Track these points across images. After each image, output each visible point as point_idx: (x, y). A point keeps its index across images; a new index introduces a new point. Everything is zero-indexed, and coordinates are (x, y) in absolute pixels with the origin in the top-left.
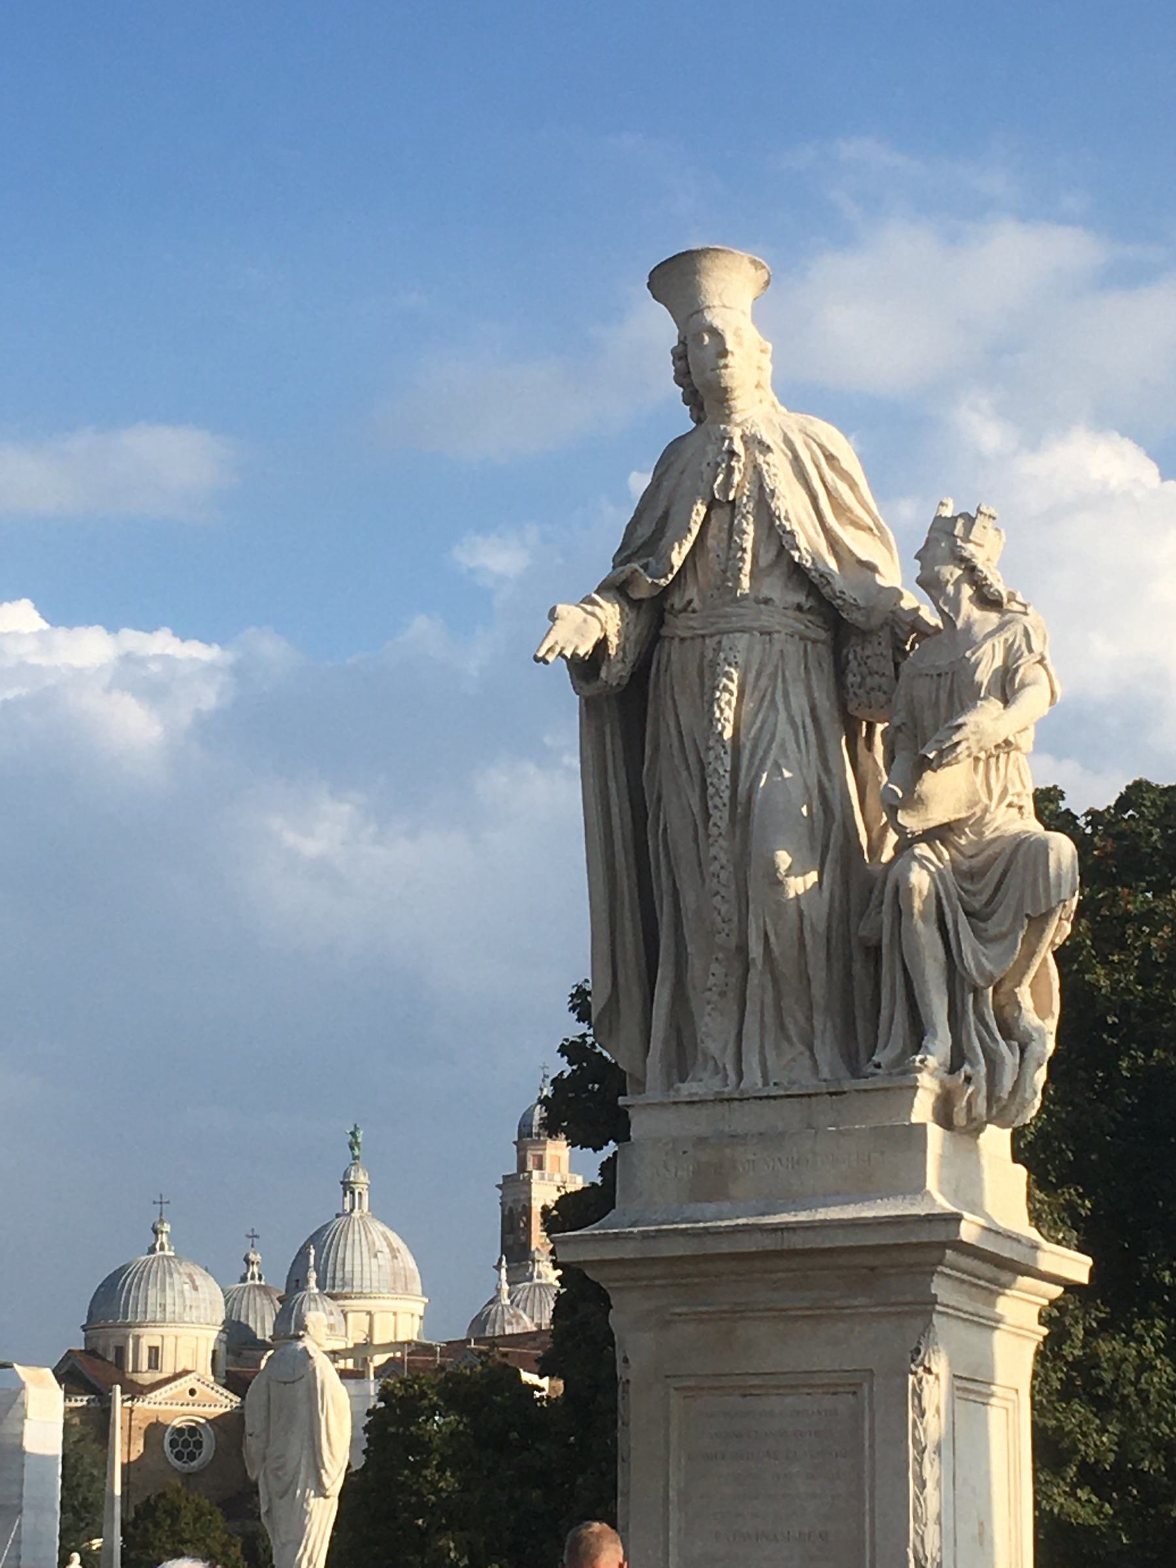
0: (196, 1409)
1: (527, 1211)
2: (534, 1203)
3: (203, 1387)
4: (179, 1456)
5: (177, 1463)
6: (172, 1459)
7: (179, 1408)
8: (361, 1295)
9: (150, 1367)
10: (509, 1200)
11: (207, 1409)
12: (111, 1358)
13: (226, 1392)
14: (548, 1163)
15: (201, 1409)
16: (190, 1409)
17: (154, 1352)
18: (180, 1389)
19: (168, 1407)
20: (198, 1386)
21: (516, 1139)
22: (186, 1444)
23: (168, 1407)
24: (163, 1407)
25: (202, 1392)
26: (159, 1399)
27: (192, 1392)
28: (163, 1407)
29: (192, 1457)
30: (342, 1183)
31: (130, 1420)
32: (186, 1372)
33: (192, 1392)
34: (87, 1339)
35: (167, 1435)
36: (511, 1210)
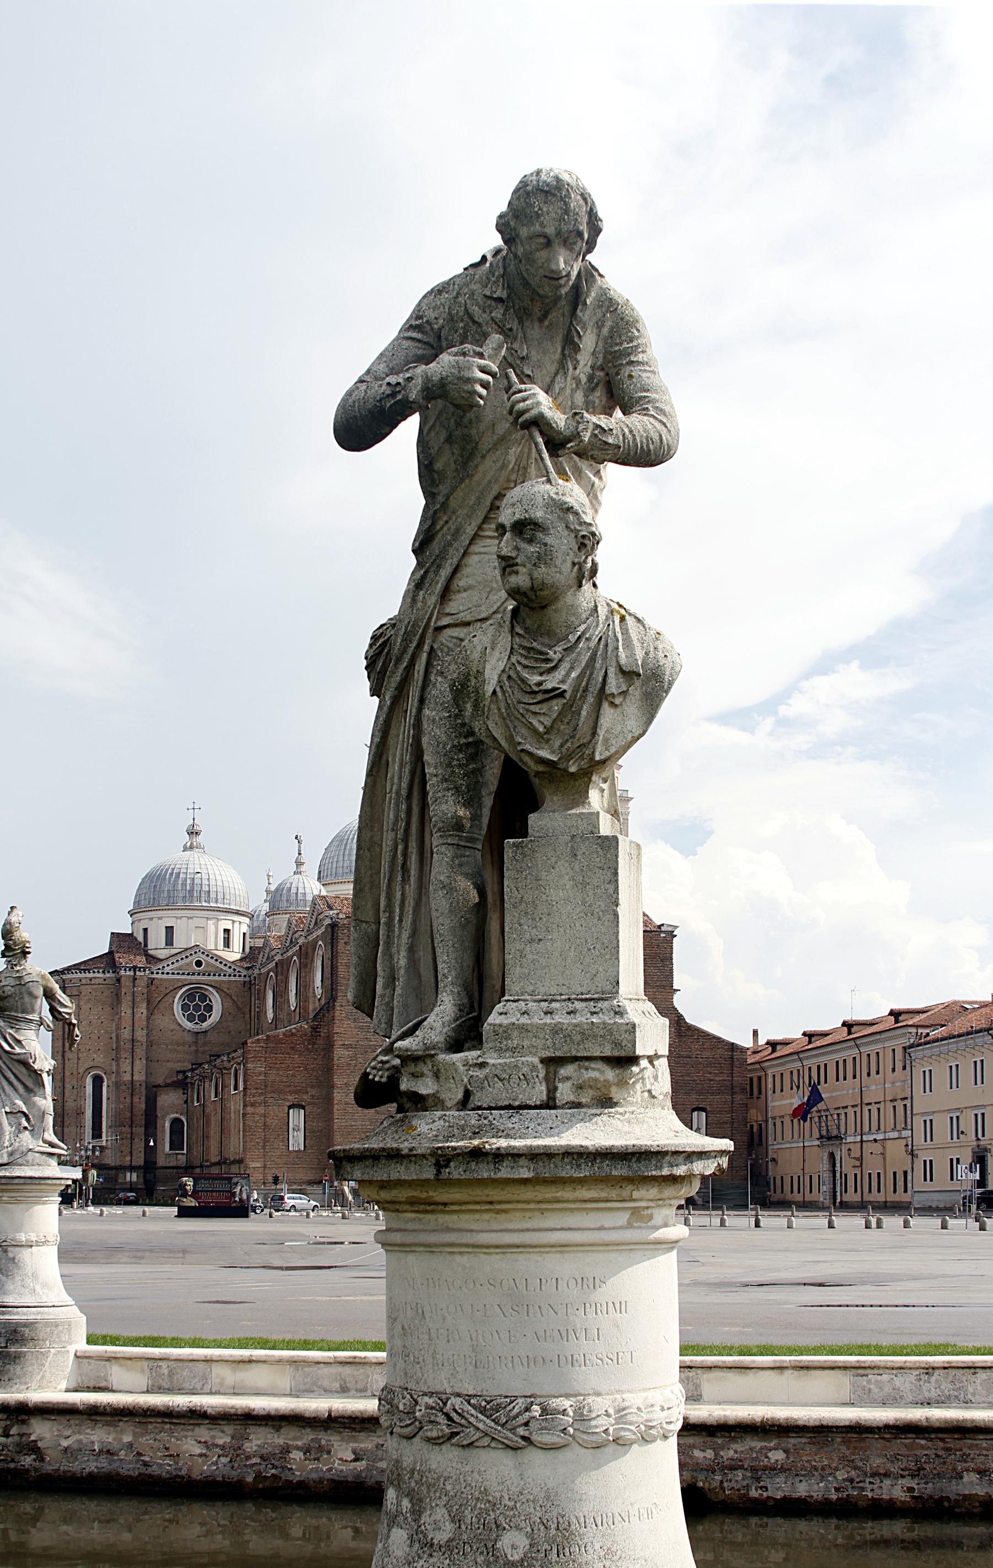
3: (208, 959)
4: (191, 1018)
5: (189, 1025)
11: (211, 978)
12: (140, 938)
15: (206, 978)
16: (196, 977)
17: (170, 930)
20: (202, 958)
22: (197, 1008)
26: (167, 969)
27: (199, 963)
29: (203, 1019)
31: (134, 986)
35: (176, 1000)
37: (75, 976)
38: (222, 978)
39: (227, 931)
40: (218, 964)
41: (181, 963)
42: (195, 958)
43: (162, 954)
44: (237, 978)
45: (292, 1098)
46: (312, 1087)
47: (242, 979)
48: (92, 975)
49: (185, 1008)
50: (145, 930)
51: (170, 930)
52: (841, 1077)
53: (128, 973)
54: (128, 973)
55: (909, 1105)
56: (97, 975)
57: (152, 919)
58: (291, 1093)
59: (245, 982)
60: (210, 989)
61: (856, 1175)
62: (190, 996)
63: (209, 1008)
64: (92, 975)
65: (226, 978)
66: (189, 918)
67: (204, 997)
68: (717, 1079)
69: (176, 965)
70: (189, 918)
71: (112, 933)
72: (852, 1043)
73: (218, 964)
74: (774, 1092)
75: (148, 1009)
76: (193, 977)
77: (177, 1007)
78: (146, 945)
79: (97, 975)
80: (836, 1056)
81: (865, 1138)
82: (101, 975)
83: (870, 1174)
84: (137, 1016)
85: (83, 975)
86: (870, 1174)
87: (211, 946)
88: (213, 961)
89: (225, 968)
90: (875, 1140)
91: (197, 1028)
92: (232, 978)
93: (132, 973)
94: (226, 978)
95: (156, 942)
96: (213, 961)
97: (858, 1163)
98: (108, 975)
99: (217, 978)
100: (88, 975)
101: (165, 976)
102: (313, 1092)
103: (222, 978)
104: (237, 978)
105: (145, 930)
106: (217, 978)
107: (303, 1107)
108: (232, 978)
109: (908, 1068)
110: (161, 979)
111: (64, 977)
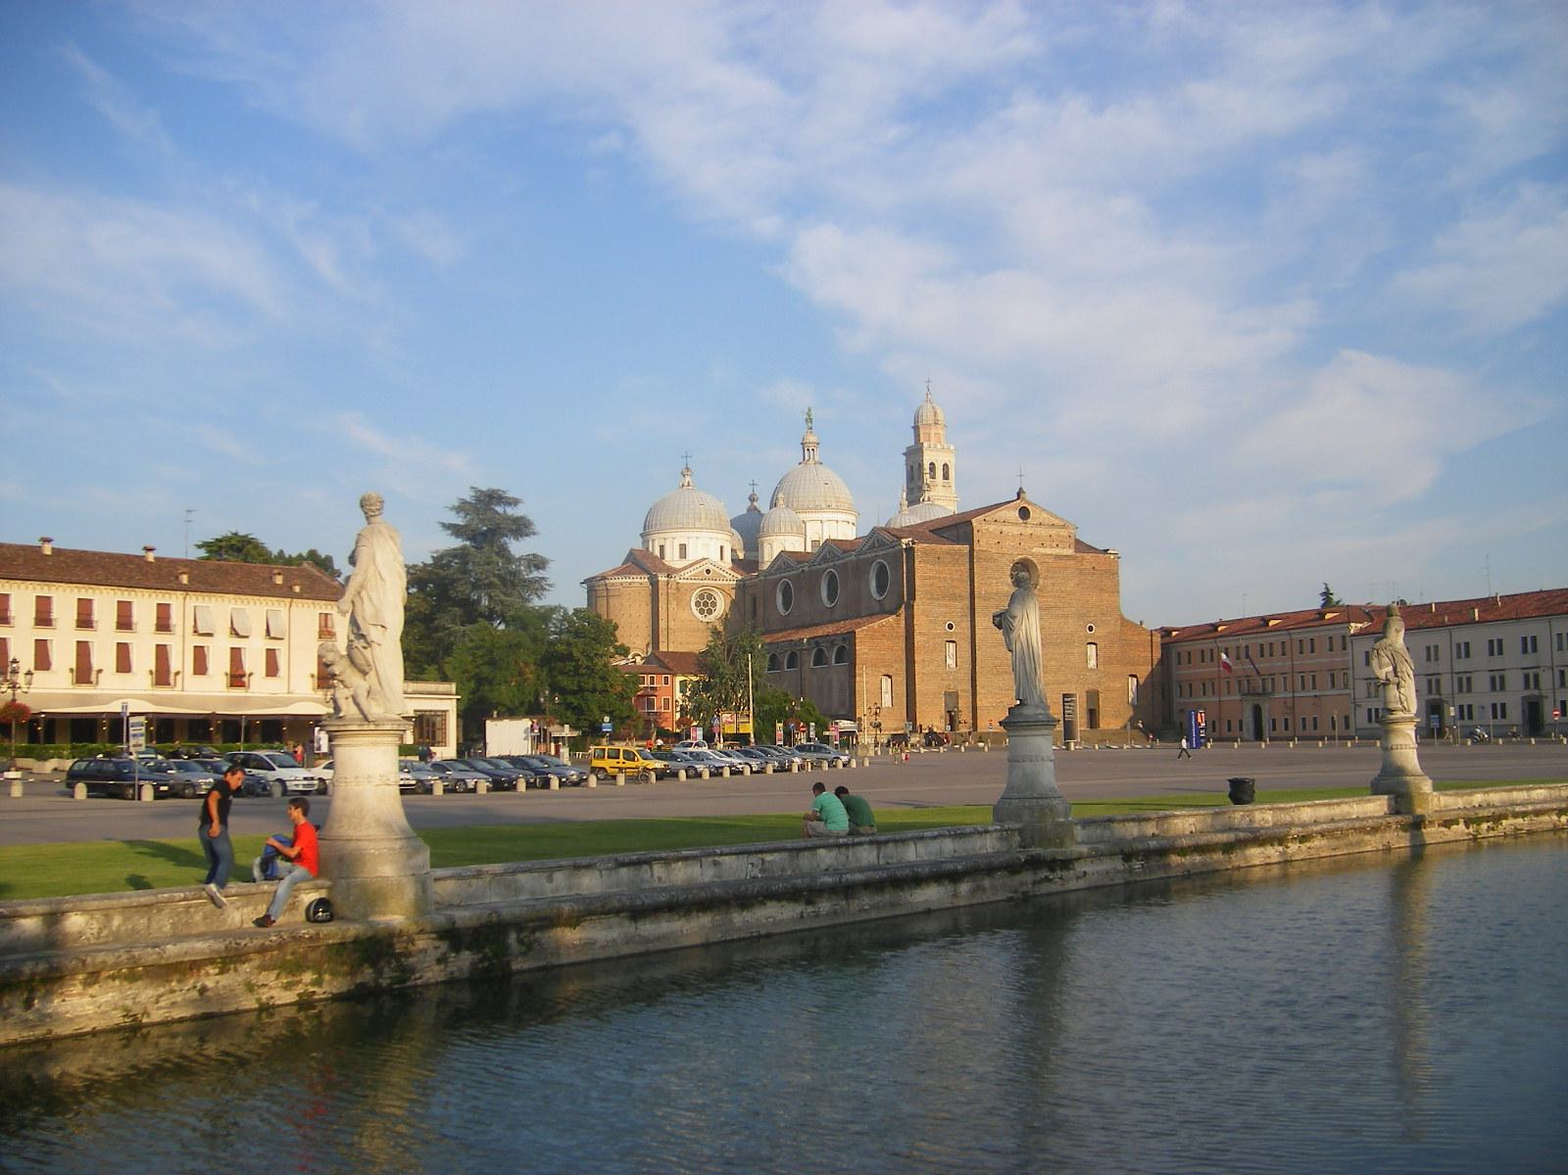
1: (921, 466)
2: (925, 462)
3: (715, 568)
4: (701, 612)
8: (817, 509)
9: (681, 557)
11: (718, 582)
12: (657, 553)
13: (733, 573)
14: (933, 436)
17: (683, 548)
18: (699, 570)
19: (694, 581)
20: (711, 567)
21: (913, 425)
22: (706, 604)
23: (694, 581)
24: (689, 581)
25: (714, 571)
26: (686, 576)
27: (708, 571)
28: (689, 581)
29: (710, 612)
35: (693, 598)
36: (912, 467)
38: (724, 582)
39: (722, 547)
40: (721, 572)
42: (705, 568)
43: (678, 564)
45: (884, 671)
46: (896, 662)
49: (697, 604)
50: (662, 548)
52: (1432, 657)
55: (1350, 672)
56: (635, 580)
58: (884, 667)
61: (1286, 720)
62: (701, 596)
63: (714, 604)
67: (710, 596)
68: (1143, 655)
69: (693, 573)
72: (1285, 632)
73: (721, 572)
74: (1179, 663)
75: (677, 605)
76: (706, 581)
77: (694, 607)
80: (1260, 641)
81: (1296, 695)
83: (1304, 719)
84: (671, 609)
85: (624, 580)
86: (1304, 719)
88: (718, 570)
89: (727, 575)
90: (1316, 696)
91: (705, 620)
95: (672, 559)
97: (1289, 711)
99: (721, 582)
101: (685, 581)
102: (896, 665)
103: (724, 582)
105: (662, 548)
107: (890, 677)
109: (1349, 649)
110: (683, 584)
111: (607, 581)
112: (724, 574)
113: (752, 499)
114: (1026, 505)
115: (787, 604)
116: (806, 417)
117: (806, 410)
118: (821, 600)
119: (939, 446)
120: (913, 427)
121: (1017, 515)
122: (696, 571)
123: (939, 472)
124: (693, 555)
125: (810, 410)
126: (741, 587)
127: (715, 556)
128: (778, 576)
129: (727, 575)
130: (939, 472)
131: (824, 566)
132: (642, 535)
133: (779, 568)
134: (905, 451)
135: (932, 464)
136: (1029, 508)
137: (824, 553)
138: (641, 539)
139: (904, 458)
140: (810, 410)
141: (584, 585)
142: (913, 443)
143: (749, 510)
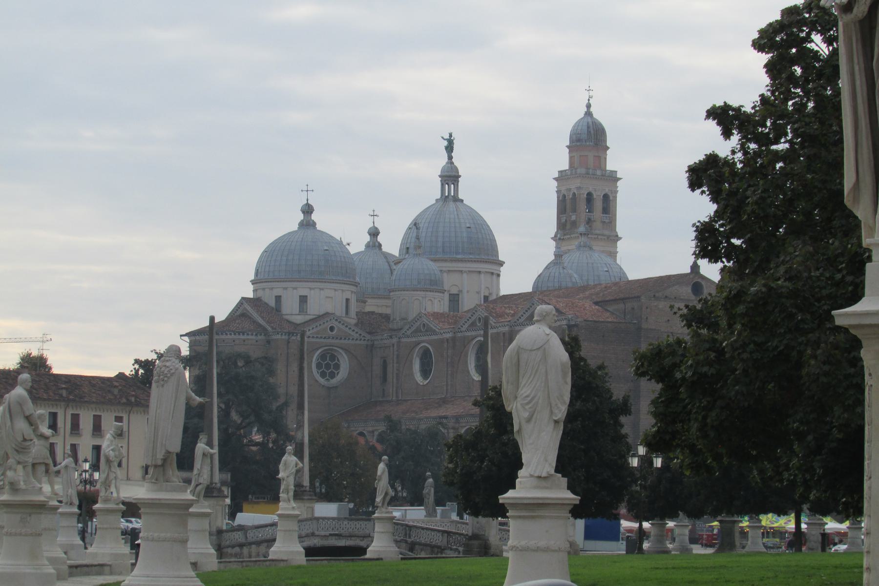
0: (334, 341)
3: (340, 325)
4: (323, 375)
5: (322, 381)
6: (318, 377)
7: (322, 340)
10: (563, 189)
11: (342, 341)
12: (272, 303)
16: (330, 341)
17: (303, 299)
20: (335, 324)
22: (328, 366)
29: (332, 375)
30: (440, 176)
31: (288, 348)
32: (327, 314)
33: (332, 329)
34: (255, 291)
36: (564, 196)
37: (229, 336)
38: (350, 342)
39: (347, 300)
41: (319, 328)
43: (299, 319)
44: (362, 342)
47: (365, 343)
48: (245, 337)
49: (319, 366)
50: (278, 299)
51: (303, 299)
53: (284, 337)
54: (284, 337)
57: (286, 289)
59: (367, 345)
60: (341, 351)
62: (323, 357)
63: (337, 367)
64: (245, 337)
65: (354, 342)
66: (321, 289)
67: (333, 357)
69: (315, 330)
70: (321, 289)
71: (243, 298)
77: (314, 366)
78: (278, 309)
79: (250, 337)
82: (253, 337)
85: (237, 337)
87: (338, 313)
88: (343, 327)
89: (352, 333)
92: (358, 342)
93: (286, 337)
94: (354, 342)
95: (290, 307)
96: (343, 327)
98: (259, 337)
100: (242, 337)
103: (350, 342)
104: (362, 342)
105: (278, 299)
106: (346, 342)
108: (358, 342)
112: (350, 332)
113: (374, 233)
114: (699, 280)
115: (425, 373)
116: (446, 143)
117: (447, 137)
118: (468, 372)
119: (599, 173)
120: (567, 147)
121: (690, 291)
122: (319, 328)
123: (598, 205)
124: (315, 308)
125: (451, 135)
126: (371, 348)
127: (340, 311)
128: (414, 339)
129: (352, 333)
130: (598, 205)
131: (473, 333)
132: (253, 282)
133: (418, 331)
134: (557, 175)
135: (589, 195)
136: (703, 283)
137: (473, 318)
138: (251, 287)
139: (555, 183)
140: (451, 135)
141: (186, 338)
142: (565, 166)
143: (368, 246)
